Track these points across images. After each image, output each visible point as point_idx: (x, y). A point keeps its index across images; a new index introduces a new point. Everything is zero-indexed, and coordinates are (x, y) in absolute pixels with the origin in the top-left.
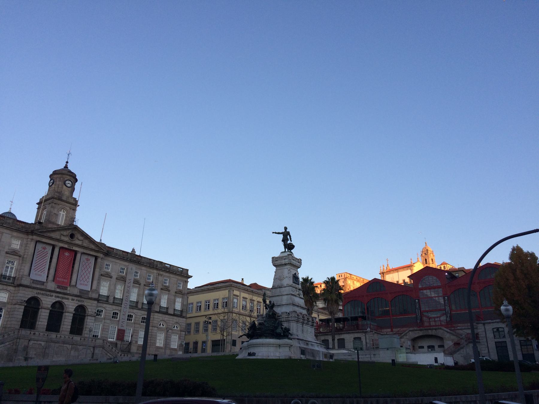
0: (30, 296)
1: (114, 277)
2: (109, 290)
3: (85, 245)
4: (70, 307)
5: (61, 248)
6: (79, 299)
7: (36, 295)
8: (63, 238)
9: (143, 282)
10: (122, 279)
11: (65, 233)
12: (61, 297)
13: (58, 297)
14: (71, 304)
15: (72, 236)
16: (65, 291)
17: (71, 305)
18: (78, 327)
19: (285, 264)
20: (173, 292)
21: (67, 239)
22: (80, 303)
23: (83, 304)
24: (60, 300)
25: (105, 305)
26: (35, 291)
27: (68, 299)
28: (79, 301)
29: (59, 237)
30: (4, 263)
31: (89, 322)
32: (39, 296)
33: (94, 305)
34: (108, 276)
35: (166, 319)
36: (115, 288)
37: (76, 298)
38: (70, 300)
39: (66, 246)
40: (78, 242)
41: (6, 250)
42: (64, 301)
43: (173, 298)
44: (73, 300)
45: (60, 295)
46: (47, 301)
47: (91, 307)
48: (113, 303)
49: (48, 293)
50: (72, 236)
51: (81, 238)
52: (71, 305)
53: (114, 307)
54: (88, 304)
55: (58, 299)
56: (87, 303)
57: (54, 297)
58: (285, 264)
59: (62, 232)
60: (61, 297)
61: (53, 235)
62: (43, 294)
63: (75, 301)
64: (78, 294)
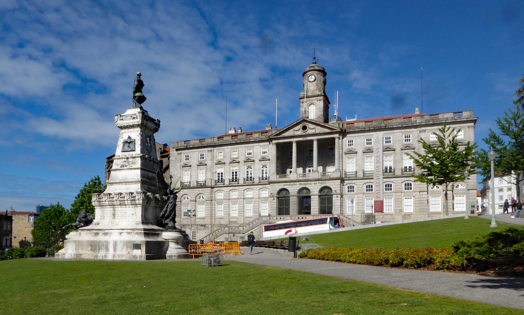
1: (360, 152)
2: (357, 165)
4: (314, 190)
5: (298, 143)
6: (320, 182)
7: (283, 187)
8: (297, 133)
9: (398, 147)
10: (368, 151)
11: (297, 128)
13: (301, 184)
14: (314, 187)
15: (304, 128)
17: (315, 189)
18: (326, 207)
22: (323, 185)
23: (326, 185)
24: (304, 186)
25: (354, 181)
26: (282, 184)
28: (321, 183)
30: (260, 168)
31: (336, 201)
32: (286, 187)
33: (337, 183)
34: (352, 152)
36: (363, 162)
37: (318, 182)
38: (313, 185)
40: (310, 132)
41: (259, 158)
42: (307, 186)
44: (315, 184)
46: (293, 189)
47: (335, 186)
48: (364, 176)
49: (292, 183)
52: (315, 189)
53: (366, 181)
54: (331, 184)
55: (301, 186)
56: (328, 184)
57: (298, 185)
59: (295, 128)
63: (318, 184)
64: (320, 177)
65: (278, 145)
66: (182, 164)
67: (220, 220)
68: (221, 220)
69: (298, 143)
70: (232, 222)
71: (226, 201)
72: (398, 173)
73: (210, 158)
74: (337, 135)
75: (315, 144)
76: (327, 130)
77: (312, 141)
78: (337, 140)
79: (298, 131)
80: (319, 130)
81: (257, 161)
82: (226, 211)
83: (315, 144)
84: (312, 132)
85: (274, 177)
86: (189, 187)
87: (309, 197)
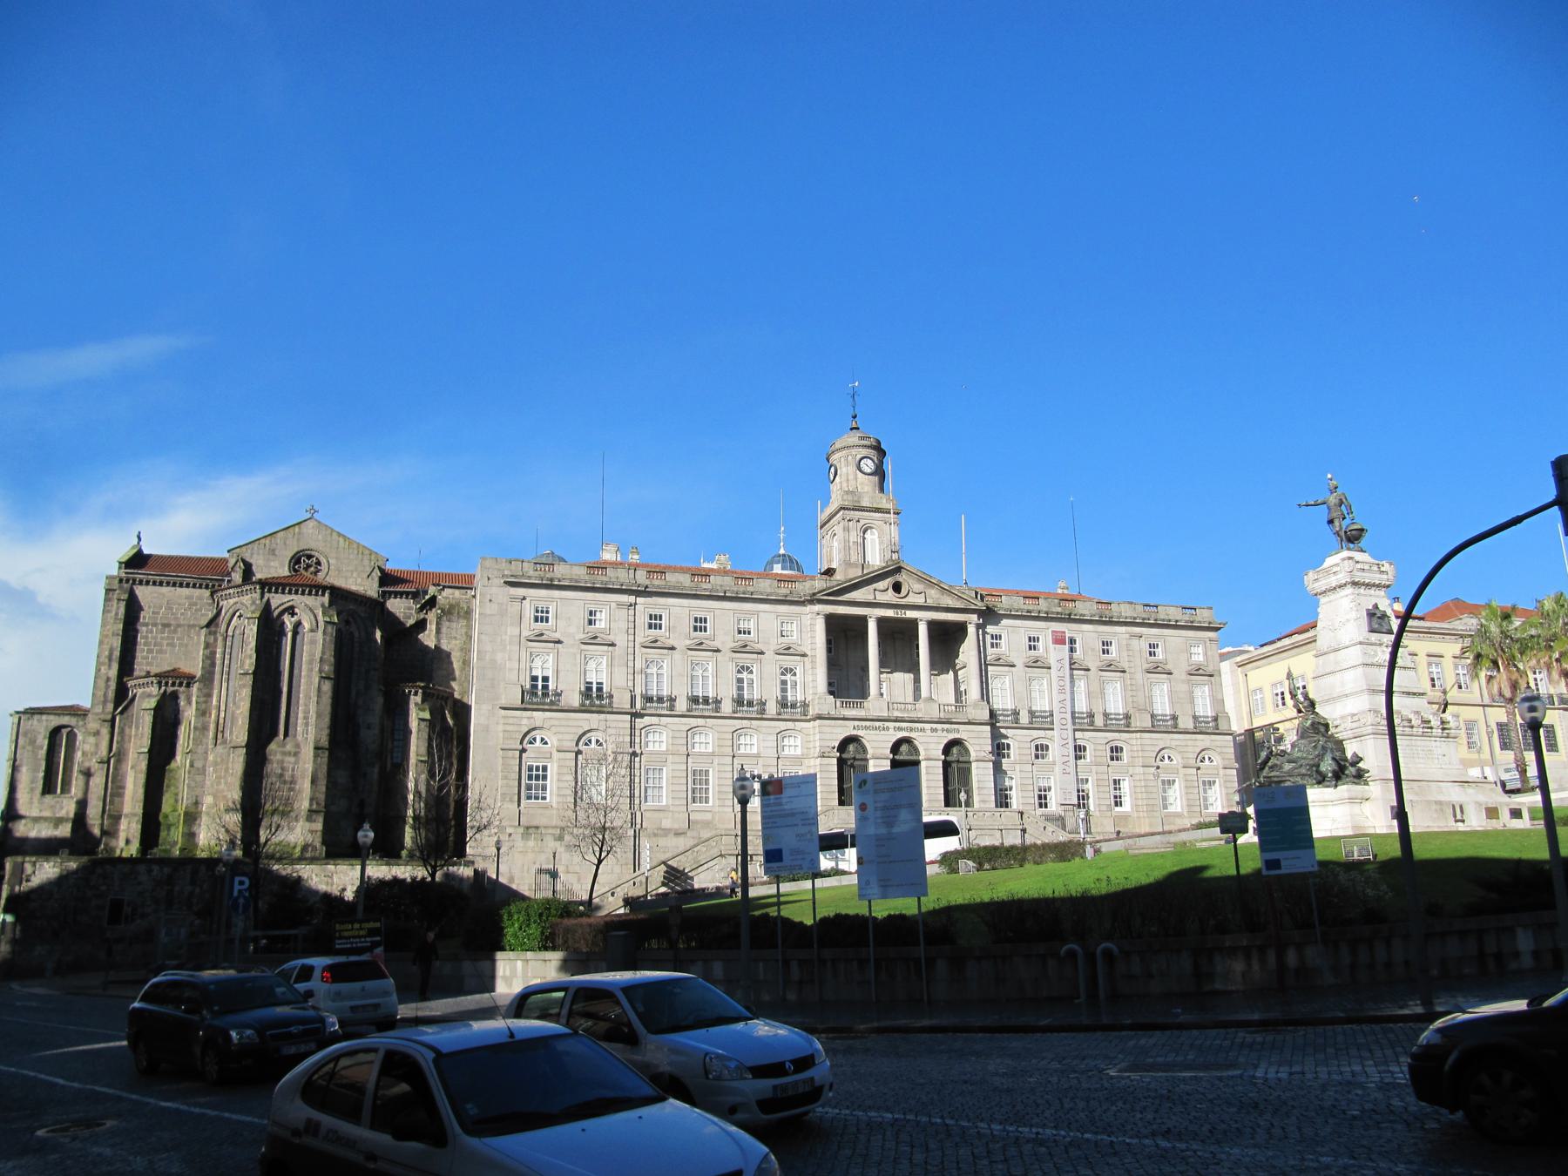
0: (841, 737)
1: (1019, 663)
3: (930, 602)
5: (881, 621)
7: (855, 733)
11: (881, 585)
12: (906, 729)
13: (900, 729)
16: (913, 715)
19: (1378, 586)
20: (1180, 673)
21: (890, 596)
22: (951, 736)
23: (956, 736)
27: (922, 730)
29: (870, 598)
32: (860, 733)
35: (1174, 743)
39: (890, 613)
43: (1184, 687)
44: (933, 730)
45: (904, 725)
50: (897, 587)
51: (917, 587)
56: (963, 733)
58: (1378, 586)
60: (906, 729)
61: (856, 595)
62: (867, 728)
65: (830, 620)
66: (525, 633)
67: (656, 815)
68: (661, 815)
69: (881, 621)
70: (697, 822)
71: (677, 759)
72: (1186, 722)
73: (624, 625)
74: (974, 617)
75: (923, 630)
76: (959, 605)
77: (914, 623)
78: (971, 629)
79: (882, 592)
80: (934, 597)
81: (769, 655)
82: (676, 788)
83: (923, 630)
84: (920, 600)
85: (829, 704)
86: (555, 707)
87: (917, 763)
